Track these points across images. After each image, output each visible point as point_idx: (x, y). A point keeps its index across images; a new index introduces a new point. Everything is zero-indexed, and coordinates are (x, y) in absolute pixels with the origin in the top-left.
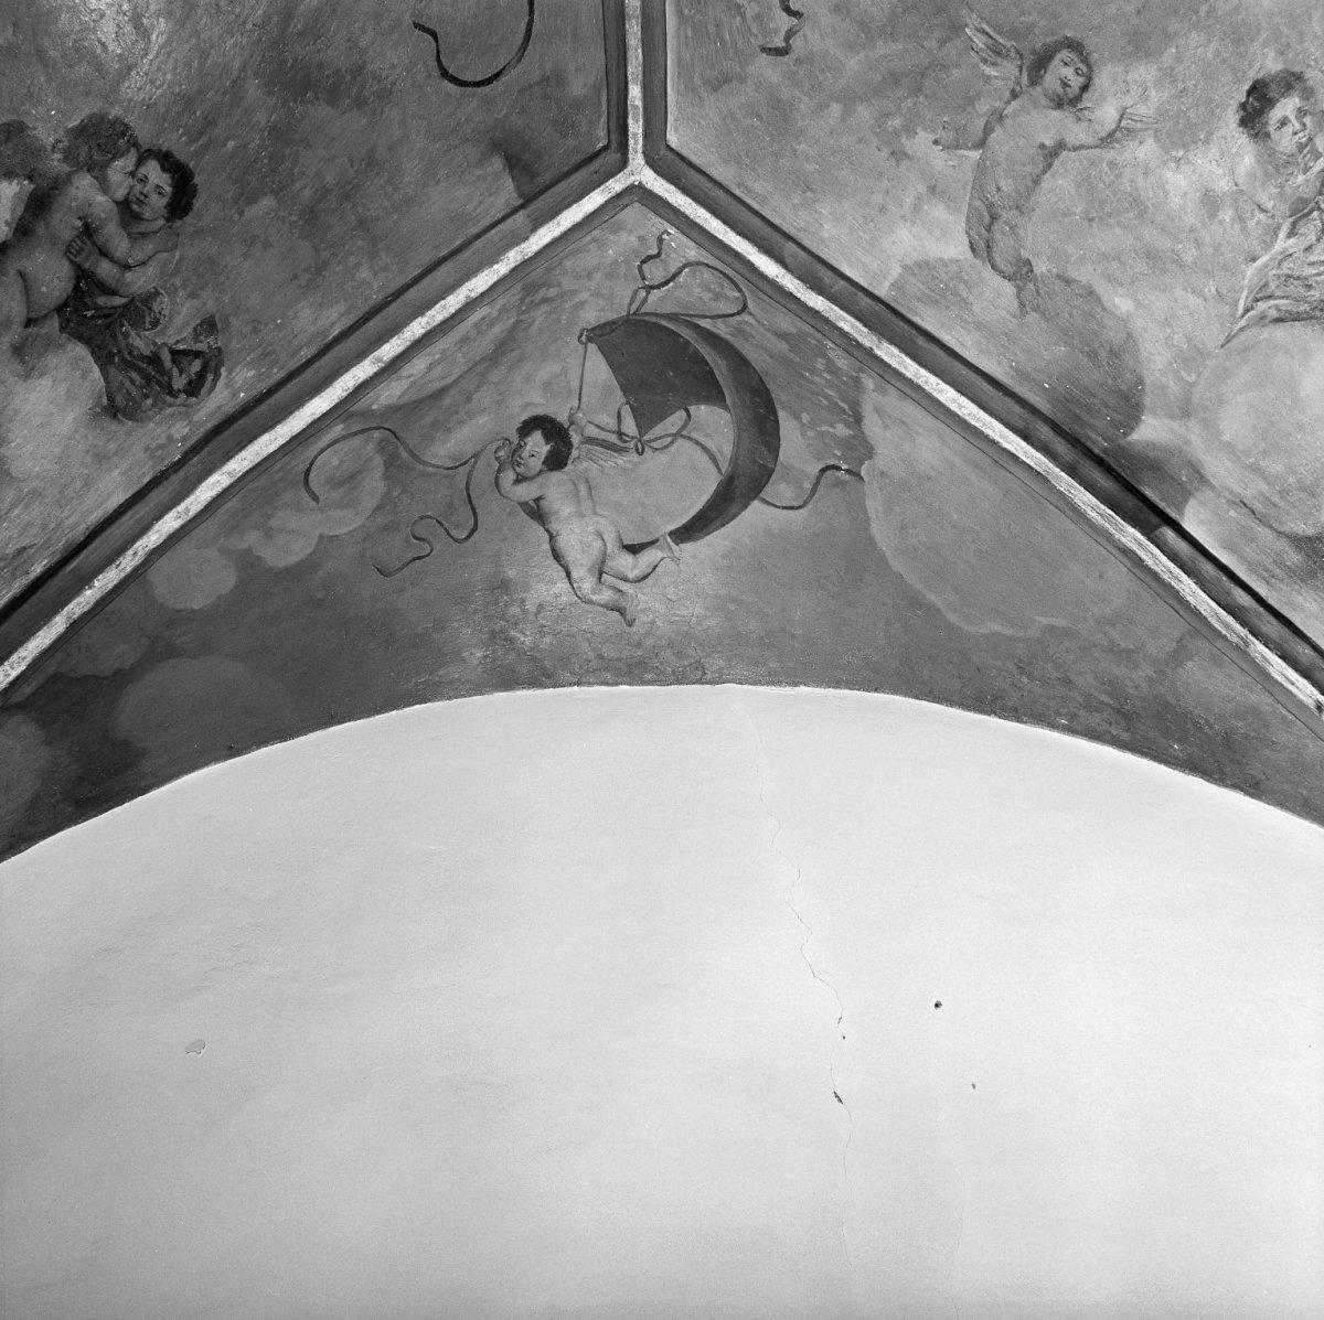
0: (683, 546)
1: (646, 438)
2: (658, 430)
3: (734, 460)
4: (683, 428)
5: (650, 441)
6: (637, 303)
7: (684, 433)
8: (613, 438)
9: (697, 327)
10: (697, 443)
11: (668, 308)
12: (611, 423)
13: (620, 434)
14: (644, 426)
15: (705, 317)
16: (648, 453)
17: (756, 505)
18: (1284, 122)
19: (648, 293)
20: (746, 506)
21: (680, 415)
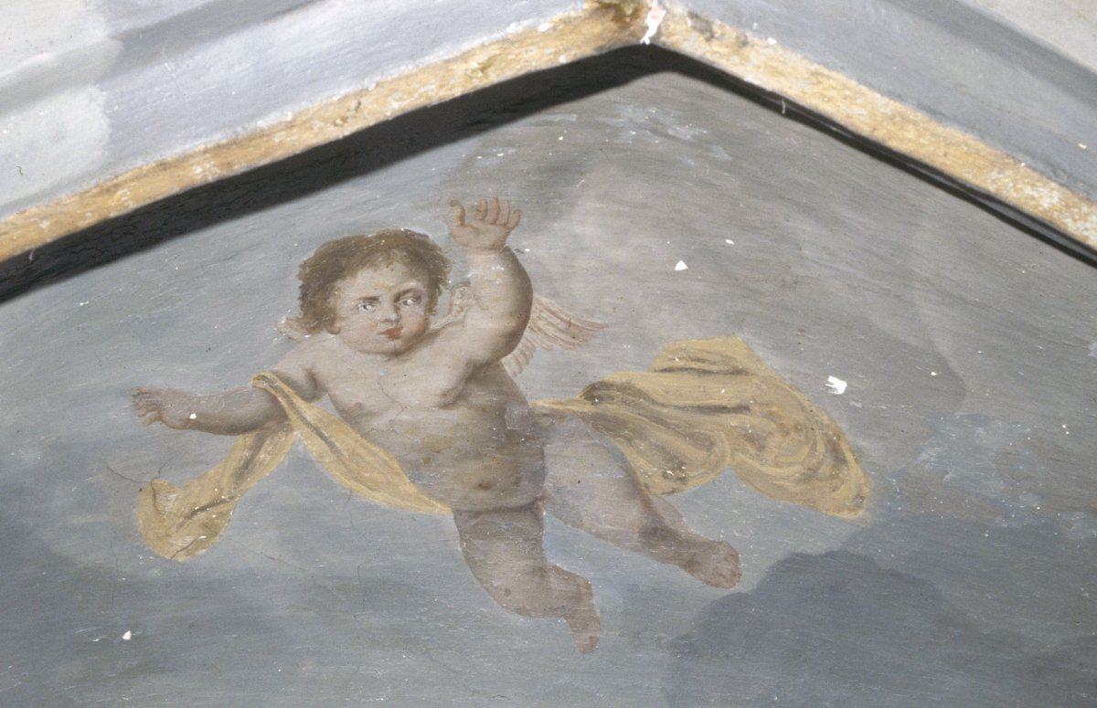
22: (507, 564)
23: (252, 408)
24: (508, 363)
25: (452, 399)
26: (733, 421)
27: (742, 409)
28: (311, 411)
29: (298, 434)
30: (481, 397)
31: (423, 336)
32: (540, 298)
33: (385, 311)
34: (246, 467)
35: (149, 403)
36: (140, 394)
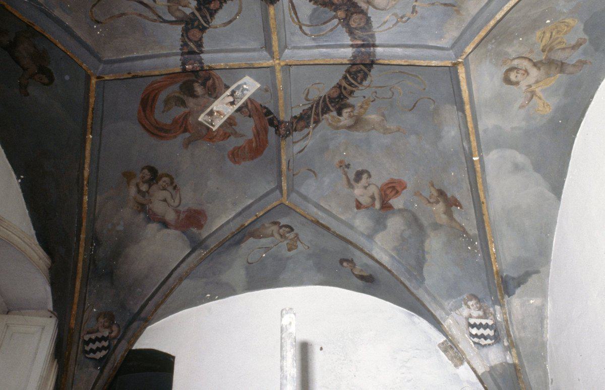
22: (571, 69)
23: (529, 95)
24: (535, 61)
25: (539, 69)
26: (554, 34)
27: (552, 33)
28: (533, 87)
29: (537, 90)
30: (539, 65)
31: (526, 71)
32: (524, 55)
33: (519, 75)
34: (540, 98)
35: (522, 107)
36: (520, 108)
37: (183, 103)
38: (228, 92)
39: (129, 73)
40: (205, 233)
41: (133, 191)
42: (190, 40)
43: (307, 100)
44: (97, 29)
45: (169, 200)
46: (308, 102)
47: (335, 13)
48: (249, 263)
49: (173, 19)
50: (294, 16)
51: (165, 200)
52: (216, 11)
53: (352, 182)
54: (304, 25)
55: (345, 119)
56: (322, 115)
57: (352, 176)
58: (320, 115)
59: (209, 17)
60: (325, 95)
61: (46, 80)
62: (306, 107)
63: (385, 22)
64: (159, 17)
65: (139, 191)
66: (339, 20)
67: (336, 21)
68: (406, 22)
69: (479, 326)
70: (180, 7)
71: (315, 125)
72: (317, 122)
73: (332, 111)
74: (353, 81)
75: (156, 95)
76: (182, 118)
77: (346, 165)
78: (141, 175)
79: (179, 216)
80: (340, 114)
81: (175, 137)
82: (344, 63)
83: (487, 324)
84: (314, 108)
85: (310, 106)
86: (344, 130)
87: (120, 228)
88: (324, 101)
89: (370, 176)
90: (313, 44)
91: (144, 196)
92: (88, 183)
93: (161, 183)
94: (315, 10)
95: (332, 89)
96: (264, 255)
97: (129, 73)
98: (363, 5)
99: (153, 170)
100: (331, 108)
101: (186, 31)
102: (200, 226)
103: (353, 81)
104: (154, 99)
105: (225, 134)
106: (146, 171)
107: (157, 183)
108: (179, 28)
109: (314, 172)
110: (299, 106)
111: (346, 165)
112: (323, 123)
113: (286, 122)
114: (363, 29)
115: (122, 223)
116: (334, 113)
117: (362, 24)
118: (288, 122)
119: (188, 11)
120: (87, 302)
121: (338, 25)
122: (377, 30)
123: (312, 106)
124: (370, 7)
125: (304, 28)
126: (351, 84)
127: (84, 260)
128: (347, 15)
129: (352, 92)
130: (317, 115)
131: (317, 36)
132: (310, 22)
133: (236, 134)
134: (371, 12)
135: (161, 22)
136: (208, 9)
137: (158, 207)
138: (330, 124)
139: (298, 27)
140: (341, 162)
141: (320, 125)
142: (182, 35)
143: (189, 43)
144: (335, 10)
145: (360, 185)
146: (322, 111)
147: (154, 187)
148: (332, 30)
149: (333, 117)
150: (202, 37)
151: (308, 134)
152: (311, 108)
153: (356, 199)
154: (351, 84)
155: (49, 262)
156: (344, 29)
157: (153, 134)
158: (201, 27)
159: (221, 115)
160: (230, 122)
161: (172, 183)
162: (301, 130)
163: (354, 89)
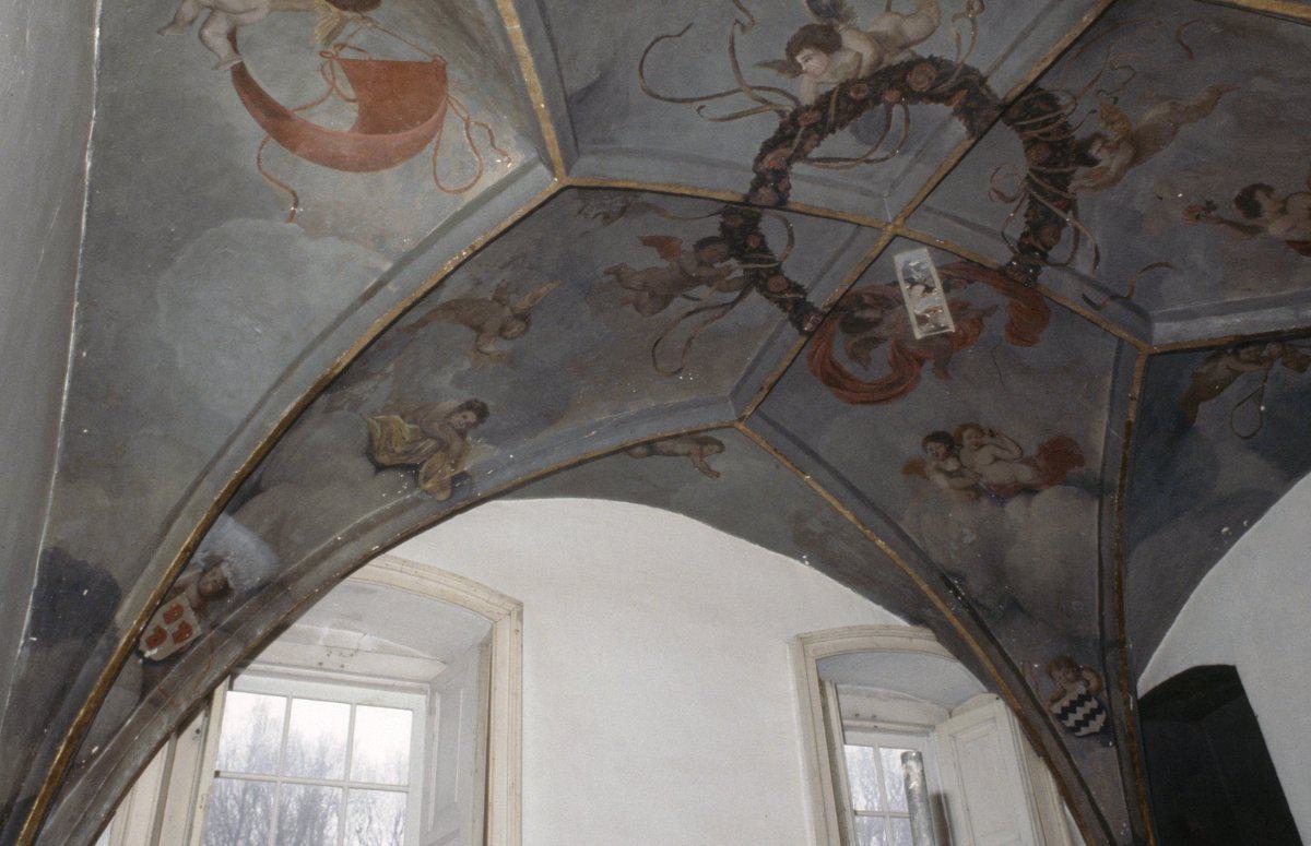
0: (229, 74)
1: (335, 63)
2: (340, 73)
3: (305, 124)
4: (339, 93)
5: (331, 65)
6: (457, 107)
7: (334, 92)
8: (341, 38)
9: (426, 140)
10: (323, 100)
11: (448, 126)
12: (352, 42)
13: (343, 46)
14: (345, 63)
15: (436, 149)
16: (320, 60)
17: (264, 133)
18: (465, 417)
19: (464, 119)
20: (264, 127)
21: (351, 94)
37: (877, 341)
38: (905, 287)
39: (762, 389)
40: (1095, 465)
41: (941, 481)
42: (781, 293)
43: (1013, 200)
44: (686, 377)
45: (998, 452)
46: (1017, 203)
47: (882, 105)
48: (1247, 438)
49: (738, 293)
50: (841, 163)
51: (996, 459)
52: (763, 243)
53: (1250, 222)
54: (870, 153)
55: (1110, 161)
56: (1066, 192)
57: (1237, 215)
58: (1064, 194)
59: (766, 257)
60: (1031, 170)
61: (716, 448)
62: (1023, 210)
63: (959, 39)
64: (723, 305)
65: (949, 475)
66: (899, 102)
67: (897, 110)
68: (982, 7)
69: (1072, 708)
70: (728, 278)
71: (1070, 212)
72: (1070, 205)
73: (1073, 172)
74: (1041, 119)
75: (833, 364)
76: (898, 354)
77: (1204, 209)
78: (930, 454)
79: (1035, 465)
80: (1093, 162)
81: (919, 377)
82: (968, 146)
83: (1071, 701)
84: (1038, 197)
85: (1027, 201)
86: (1130, 171)
87: (970, 538)
88: (1040, 175)
89: (1268, 190)
90: (909, 157)
91: (962, 476)
92: (863, 524)
93: (966, 442)
94: (855, 131)
95: (1028, 156)
96: (1262, 408)
97: (762, 389)
98: (903, 57)
99: (937, 437)
100: (1066, 170)
101: (763, 289)
102: (1080, 461)
103: (1041, 119)
104: (838, 369)
105: (973, 321)
106: (931, 445)
107: (962, 446)
108: (754, 296)
109: (1160, 264)
110: (1009, 219)
111: (1204, 209)
112: (1082, 199)
113: (1010, 264)
114: (943, 78)
115: (966, 531)
116: (1081, 170)
117: (934, 75)
118: (1014, 259)
119: (740, 273)
120: (1016, 662)
121: (906, 109)
122: (962, 57)
123: (1032, 197)
124: (913, 48)
125: (871, 157)
126: (1045, 124)
127: (956, 614)
128: (900, 89)
129: (1065, 128)
130: (1055, 198)
131: (901, 146)
132: (871, 144)
133: (987, 312)
134: (923, 51)
135: (732, 308)
136: (752, 251)
137: (997, 474)
138: (1095, 188)
139: (863, 165)
140: (1190, 210)
141: (1079, 204)
142: (767, 297)
143: (783, 297)
144: (877, 101)
145: (1266, 215)
146: (1059, 188)
147: (964, 454)
148: (907, 120)
149: (1086, 176)
150: (787, 279)
151: (1077, 231)
152: (1033, 201)
153: (1288, 242)
154: (1045, 124)
155: (928, 633)
156: (920, 103)
157: (887, 400)
158: (772, 272)
159: (935, 311)
160: (957, 309)
161: (980, 431)
162: (1058, 238)
163: (1060, 122)
